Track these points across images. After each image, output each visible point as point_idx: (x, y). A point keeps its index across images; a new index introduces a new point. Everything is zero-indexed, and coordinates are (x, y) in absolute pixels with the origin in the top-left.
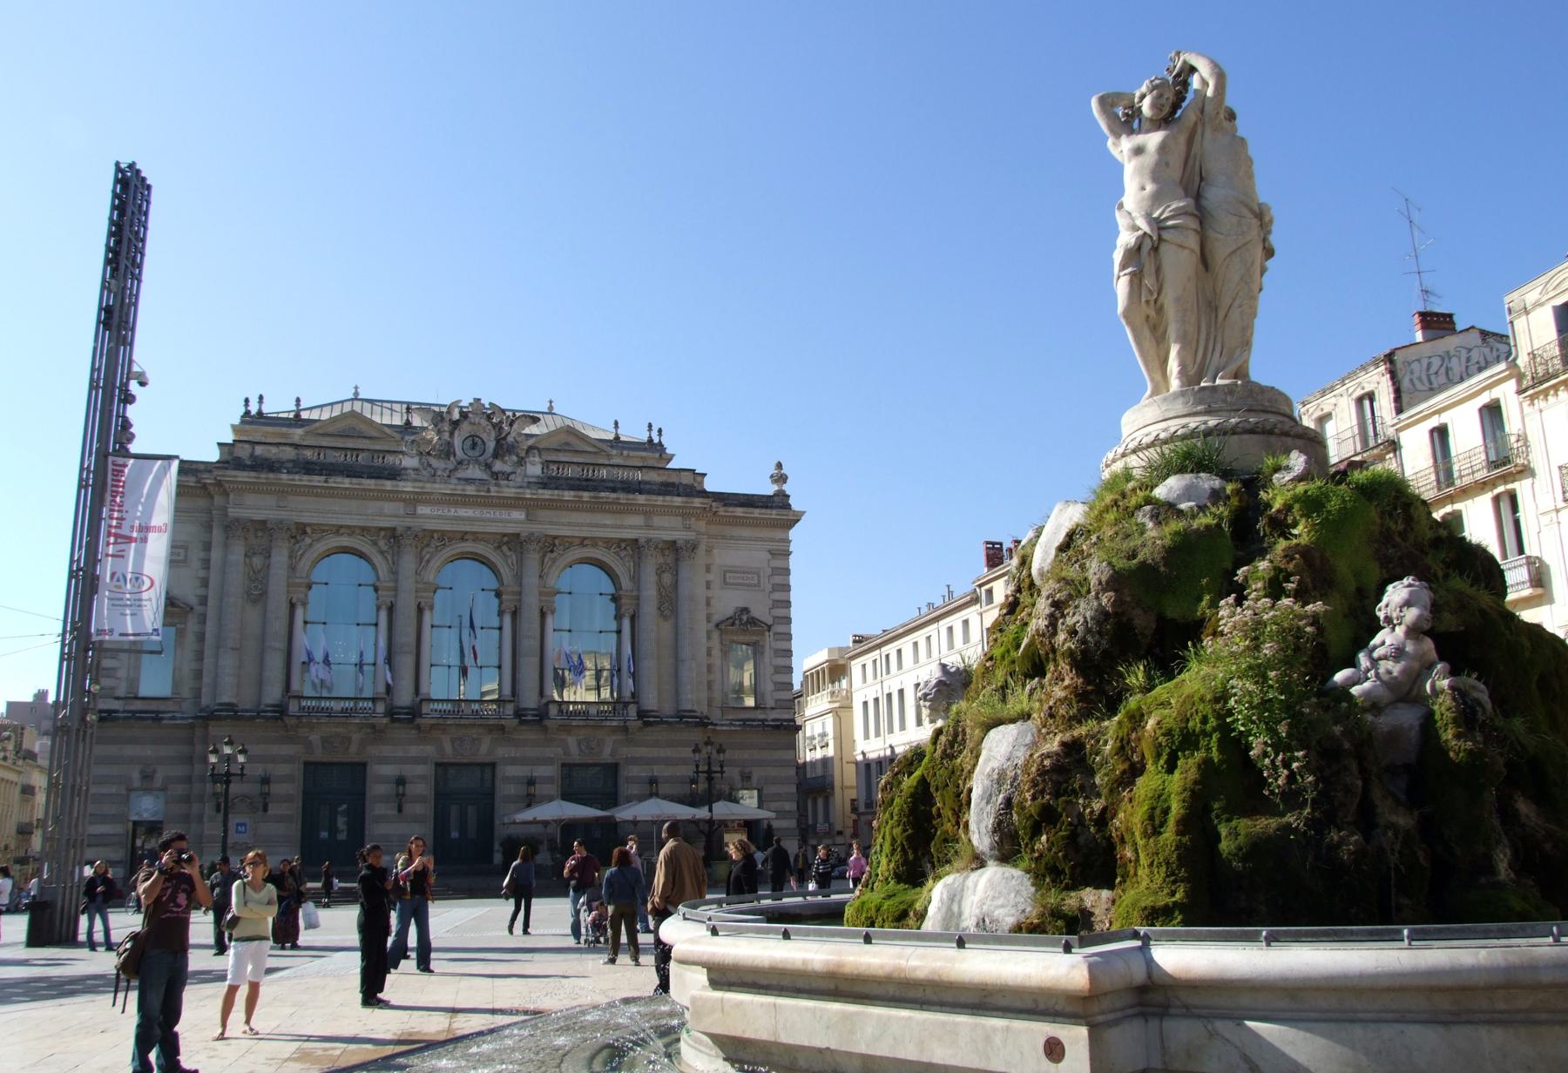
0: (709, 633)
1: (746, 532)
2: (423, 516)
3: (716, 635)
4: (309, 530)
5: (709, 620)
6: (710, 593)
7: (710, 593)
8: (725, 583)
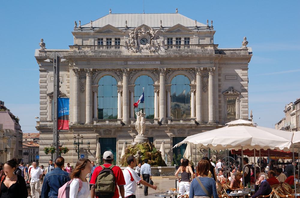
0: (220, 96)
1: (232, 62)
2: (129, 64)
3: (222, 96)
4: (97, 71)
5: (219, 91)
6: (220, 83)
7: (220, 83)
8: (226, 79)
